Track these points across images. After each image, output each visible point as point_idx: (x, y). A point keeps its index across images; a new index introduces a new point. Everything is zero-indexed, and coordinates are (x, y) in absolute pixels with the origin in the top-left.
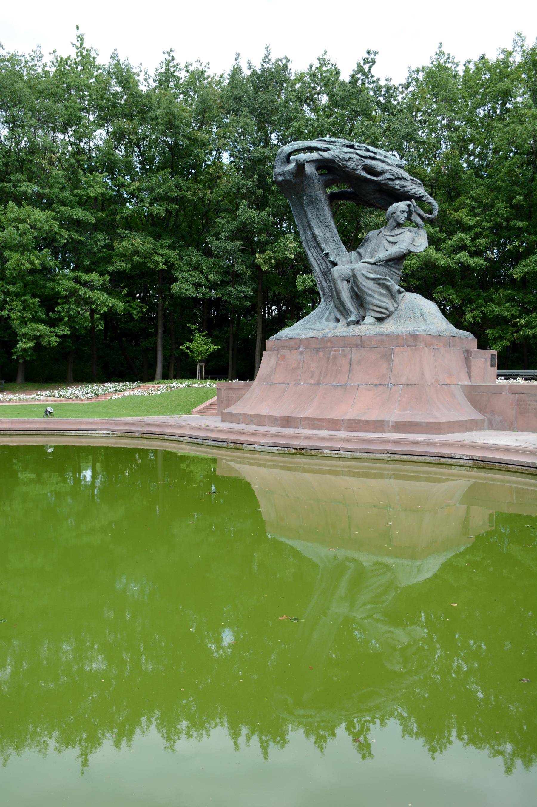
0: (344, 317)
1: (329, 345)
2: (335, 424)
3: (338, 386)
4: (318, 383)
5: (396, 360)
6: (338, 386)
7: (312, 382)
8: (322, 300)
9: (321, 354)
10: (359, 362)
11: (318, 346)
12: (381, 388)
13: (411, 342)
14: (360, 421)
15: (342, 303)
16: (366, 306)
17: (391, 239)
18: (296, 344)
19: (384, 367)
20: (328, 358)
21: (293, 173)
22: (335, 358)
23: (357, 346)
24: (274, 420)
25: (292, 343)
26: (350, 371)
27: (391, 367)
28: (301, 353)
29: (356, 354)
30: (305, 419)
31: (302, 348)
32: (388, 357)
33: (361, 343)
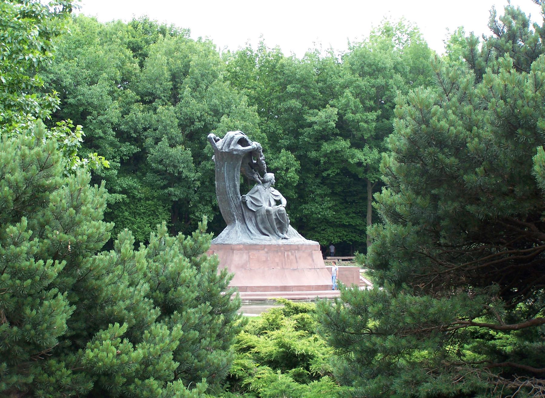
0: (270, 233)
1: (282, 248)
2: (309, 288)
3: (294, 270)
4: (283, 268)
5: (314, 257)
6: (294, 270)
7: (279, 268)
8: (237, 221)
9: (280, 254)
10: (300, 258)
11: (276, 249)
12: (313, 270)
13: (317, 249)
14: (319, 286)
15: (272, 226)
16: (284, 229)
17: (273, 193)
18: (261, 247)
19: (310, 260)
20: (284, 255)
21: (244, 152)
22: (288, 255)
23: (296, 250)
24: (276, 288)
25: (258, 247)
26: (297, 262)
27: (313, 260)
28: (267, 253)
29: (298, 254)
30: (295, 286)
31: (266, 250)
32: (311, 255)
33: (298, 248)
